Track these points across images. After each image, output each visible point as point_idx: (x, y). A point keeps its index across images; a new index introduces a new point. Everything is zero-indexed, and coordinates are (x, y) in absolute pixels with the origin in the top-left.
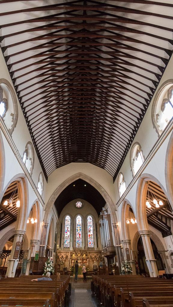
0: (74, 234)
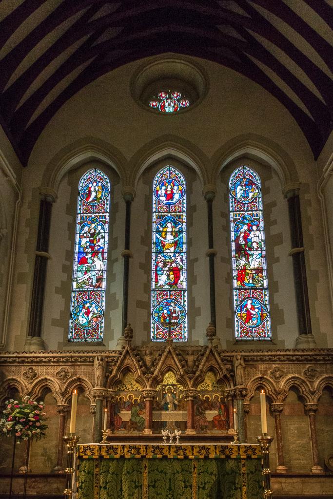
0: (134, 263)
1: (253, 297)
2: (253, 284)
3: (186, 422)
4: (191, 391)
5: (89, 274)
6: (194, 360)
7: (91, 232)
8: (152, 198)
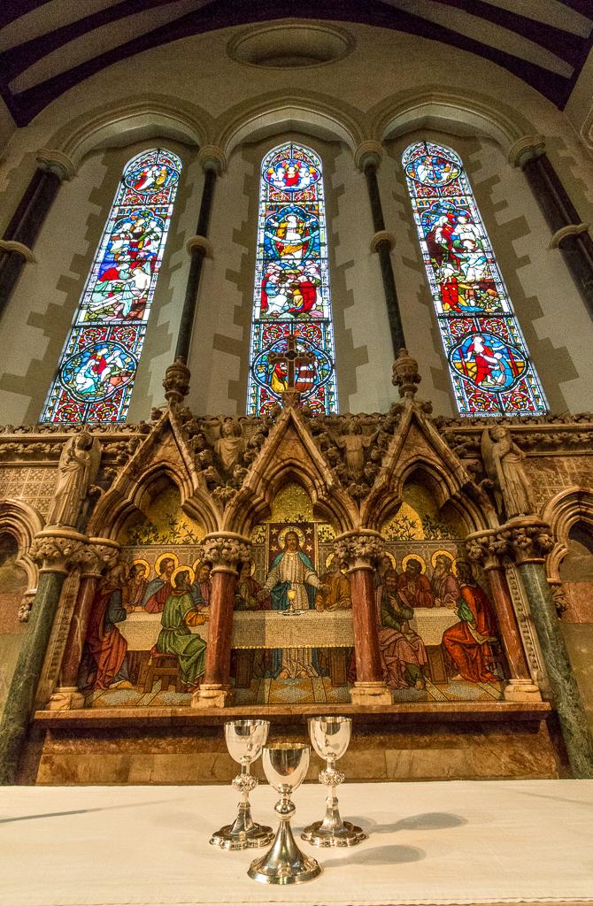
1: (484, 331)
2: (479, 307)
3: (348, 654)
4: (361, 539)
5: (118, 297)
6: (364, 448)
7: (135, 231)
8: (258, 183)
